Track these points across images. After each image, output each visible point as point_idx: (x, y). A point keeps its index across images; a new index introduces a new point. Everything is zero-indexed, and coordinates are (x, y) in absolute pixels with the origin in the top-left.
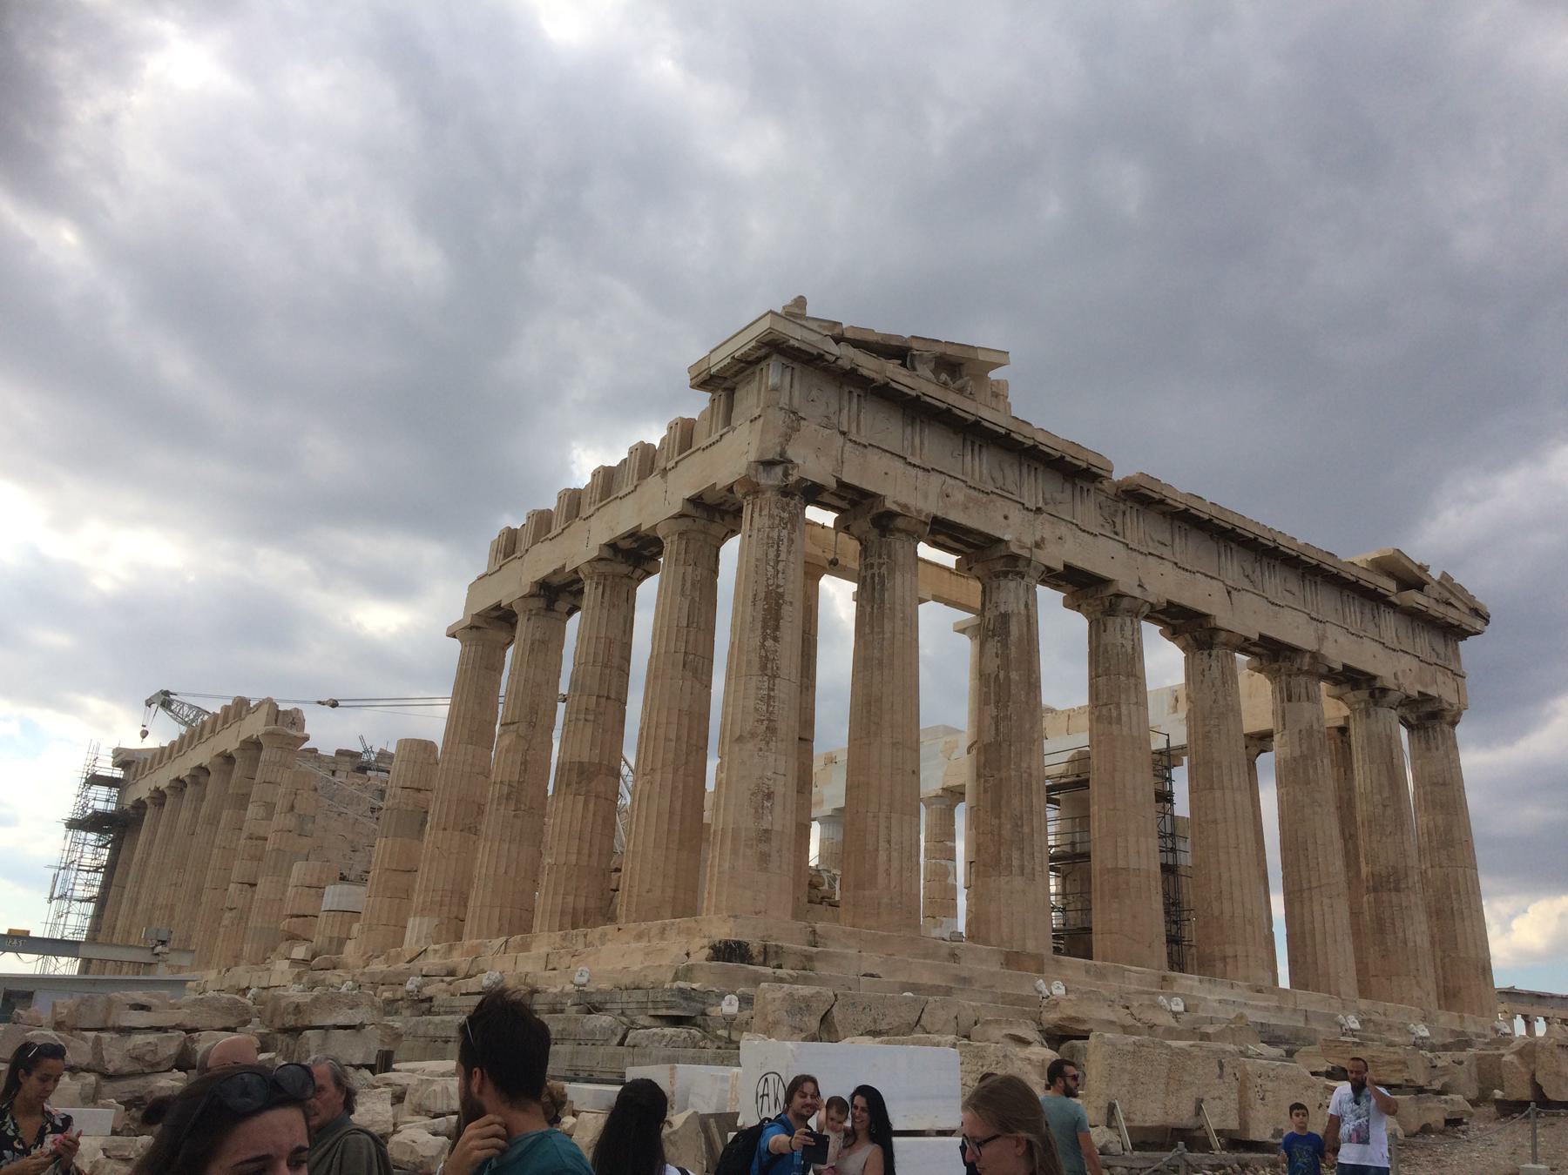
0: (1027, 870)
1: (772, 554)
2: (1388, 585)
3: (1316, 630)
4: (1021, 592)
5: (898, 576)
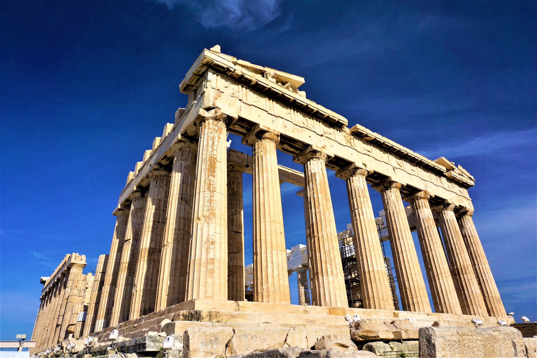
0: (334, 273)
1: (210, 142)
2: (443, 169)
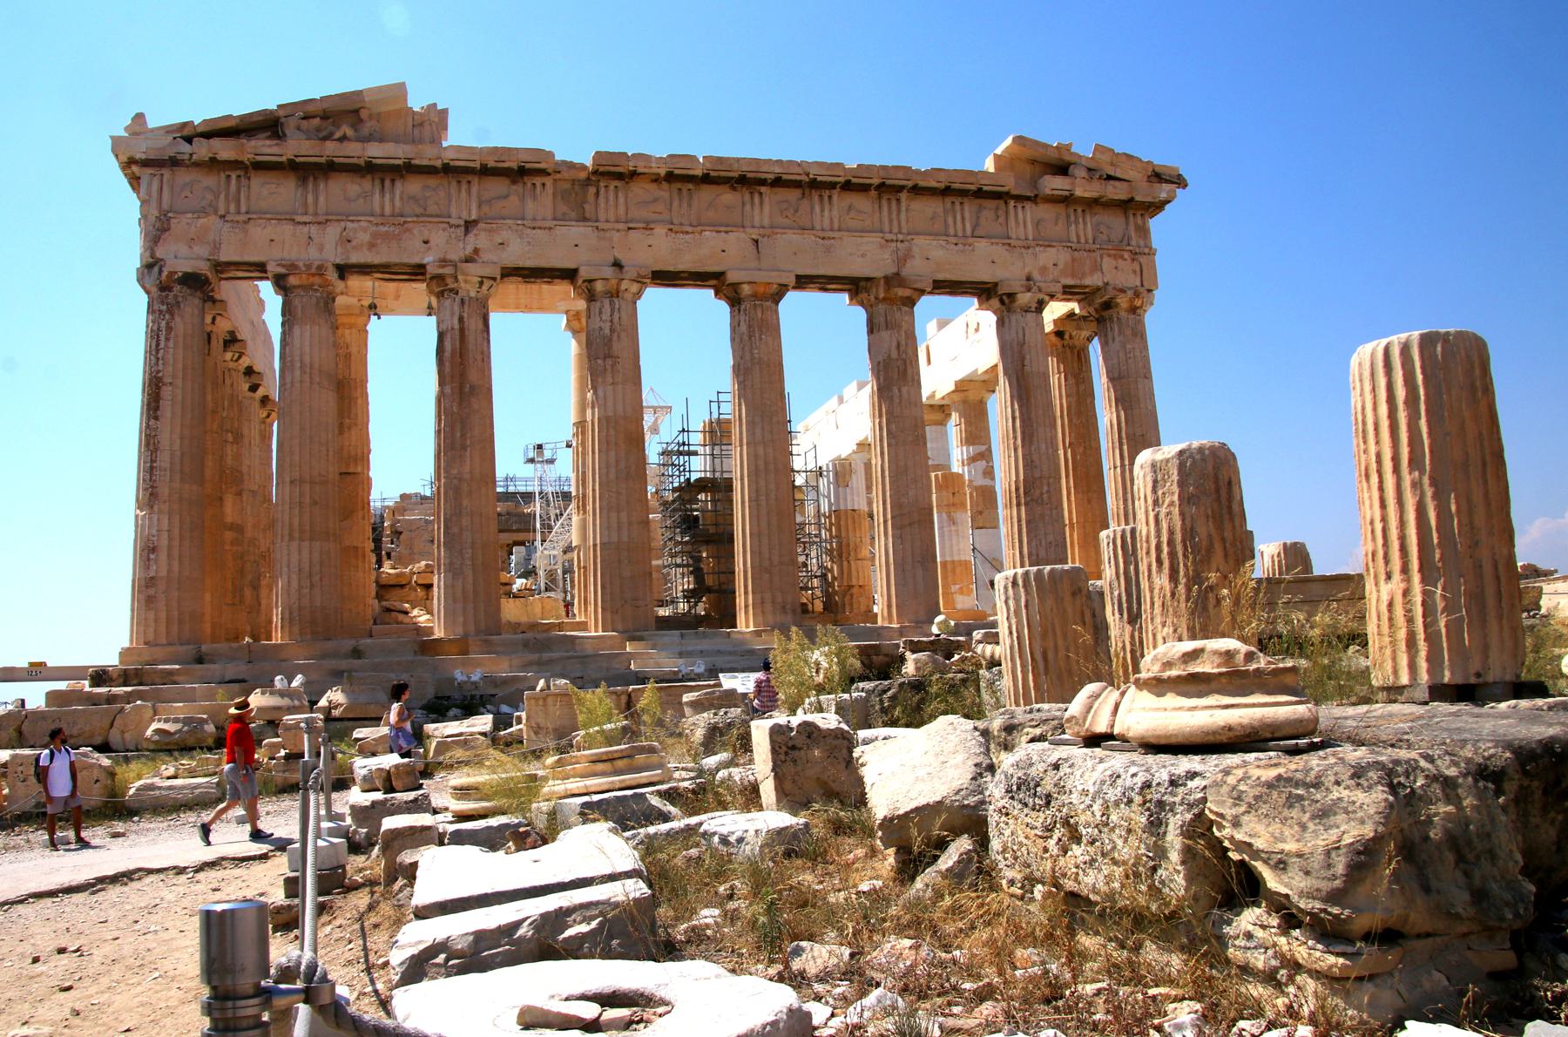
4: (456, 308)
5: (297, 330)
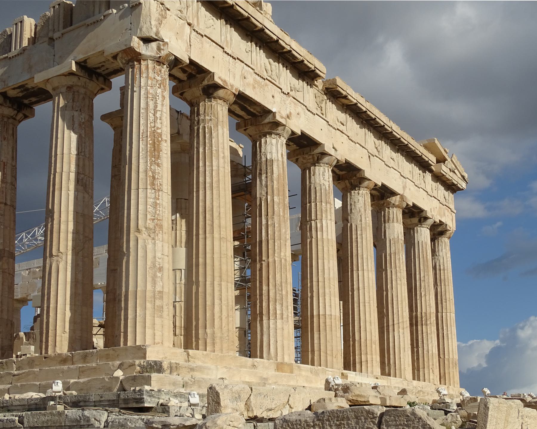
3: (403, 182)
